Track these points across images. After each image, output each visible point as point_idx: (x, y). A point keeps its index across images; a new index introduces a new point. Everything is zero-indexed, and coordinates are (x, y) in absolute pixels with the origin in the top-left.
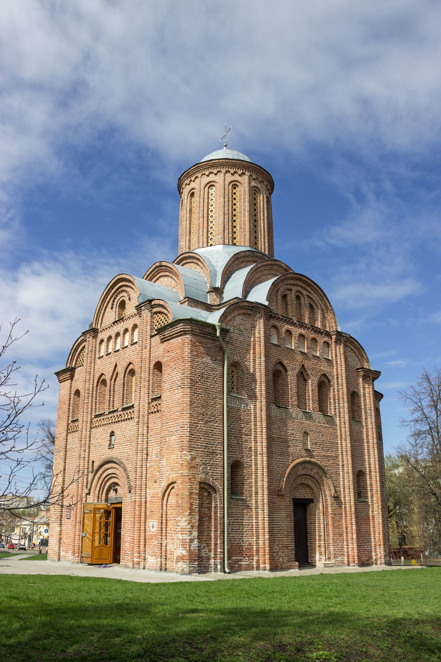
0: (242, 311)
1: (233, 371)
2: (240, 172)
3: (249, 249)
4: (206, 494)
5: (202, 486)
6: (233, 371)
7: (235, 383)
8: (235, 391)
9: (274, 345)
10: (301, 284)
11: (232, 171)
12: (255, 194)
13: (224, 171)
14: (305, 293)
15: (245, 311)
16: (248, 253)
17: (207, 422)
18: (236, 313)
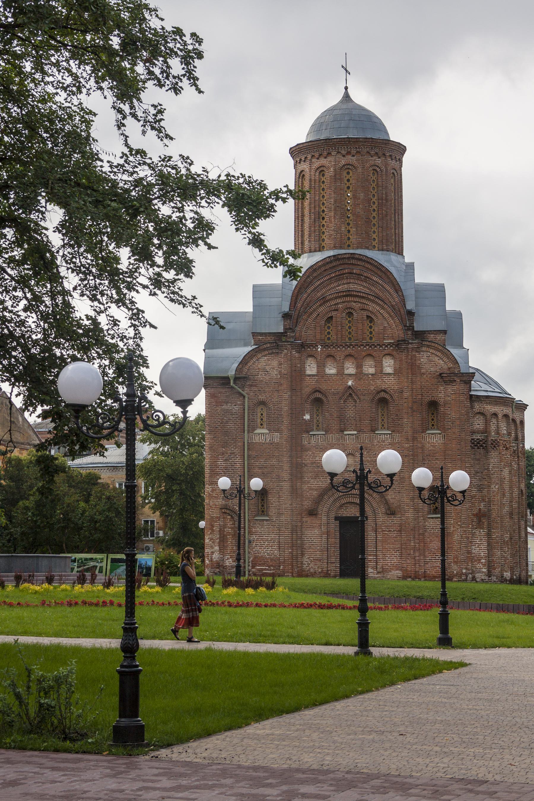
0: (263, 354)
1: (262, 409)
2: (325, 153)
3: (331, 253)
4: (229, 517)
5: (223, 511)
6: (262, 409)
7: (265, 419)
8: (265, 426)
9: (309, 375)
10: (352, 299)
11: (317, 155)
12: (348, 173)
13: (309, 156)
14: (356, 306)
15: (270, 351)
16: (328, 260)
17: (226, 460)
18: (259, 355)
